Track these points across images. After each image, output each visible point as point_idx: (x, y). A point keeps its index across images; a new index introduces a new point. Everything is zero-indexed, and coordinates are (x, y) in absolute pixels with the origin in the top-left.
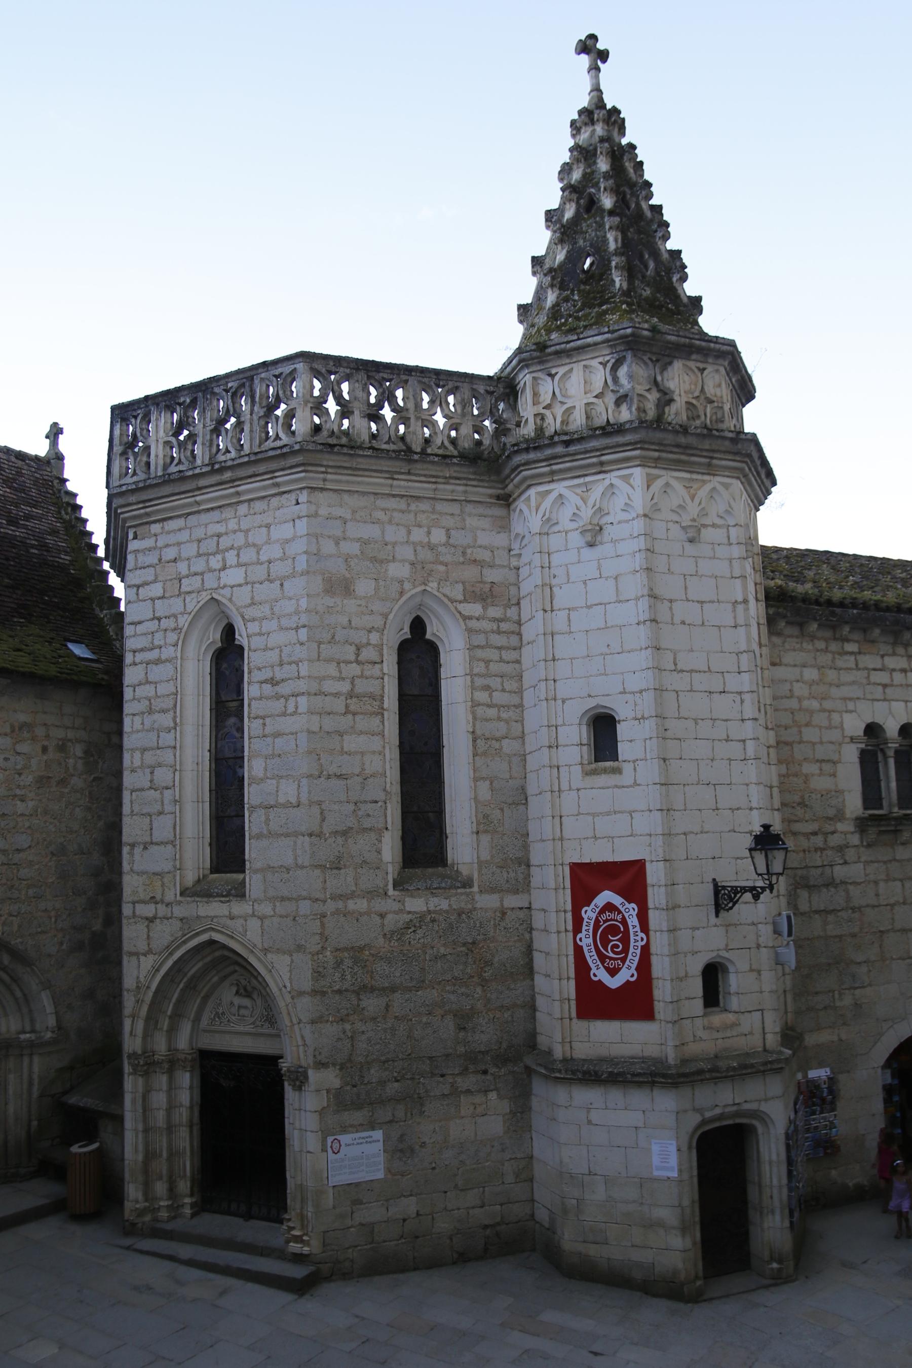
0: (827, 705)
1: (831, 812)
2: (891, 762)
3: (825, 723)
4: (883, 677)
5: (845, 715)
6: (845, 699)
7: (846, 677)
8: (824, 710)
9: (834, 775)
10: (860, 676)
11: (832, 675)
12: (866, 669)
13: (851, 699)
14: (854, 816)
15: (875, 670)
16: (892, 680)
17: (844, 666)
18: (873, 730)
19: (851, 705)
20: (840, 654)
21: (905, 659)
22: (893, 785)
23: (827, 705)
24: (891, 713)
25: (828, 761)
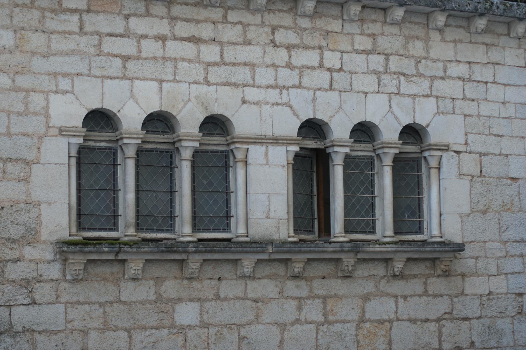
0: (23, 81)
1: (15, 232)
2: (131, 165)
3: (21, 108)
4: (127, 47)
5: (53, 97)
6: (55, 75)
7: (59, 44)
8: (19, 90)
9: (27, 180)
10: (85, 43)
11: (37, 40)
12: (98, 33)
13: (65, 75)
14: (54, 238)
15: (111, 35)
16: (140, 51)
17: (60, 28)
18: (313, 128)
19: (64, 84)
20: (53, 11)
21: (165, 22)
22: (131, 196)
23: (23, 81)
24: (132, 96)
25: (17, 160)
